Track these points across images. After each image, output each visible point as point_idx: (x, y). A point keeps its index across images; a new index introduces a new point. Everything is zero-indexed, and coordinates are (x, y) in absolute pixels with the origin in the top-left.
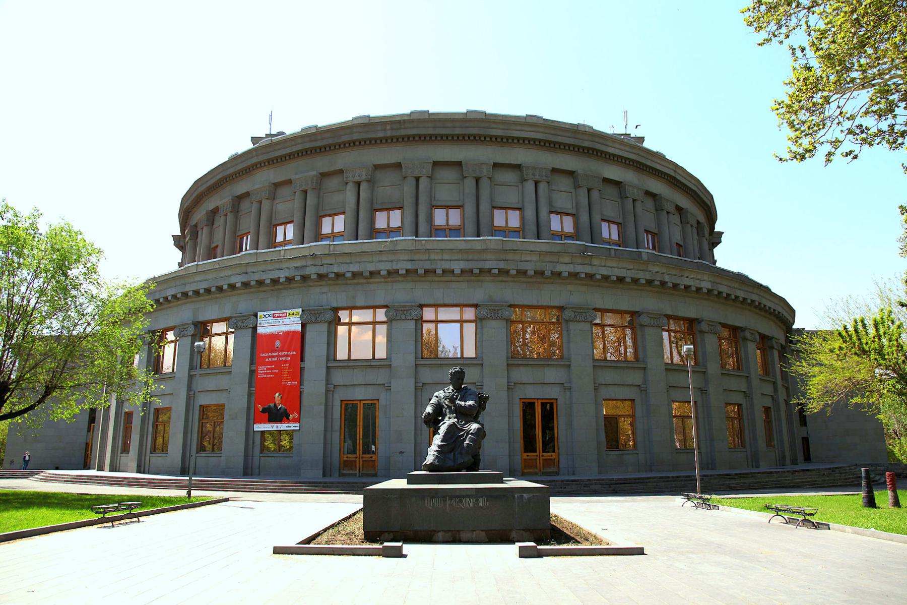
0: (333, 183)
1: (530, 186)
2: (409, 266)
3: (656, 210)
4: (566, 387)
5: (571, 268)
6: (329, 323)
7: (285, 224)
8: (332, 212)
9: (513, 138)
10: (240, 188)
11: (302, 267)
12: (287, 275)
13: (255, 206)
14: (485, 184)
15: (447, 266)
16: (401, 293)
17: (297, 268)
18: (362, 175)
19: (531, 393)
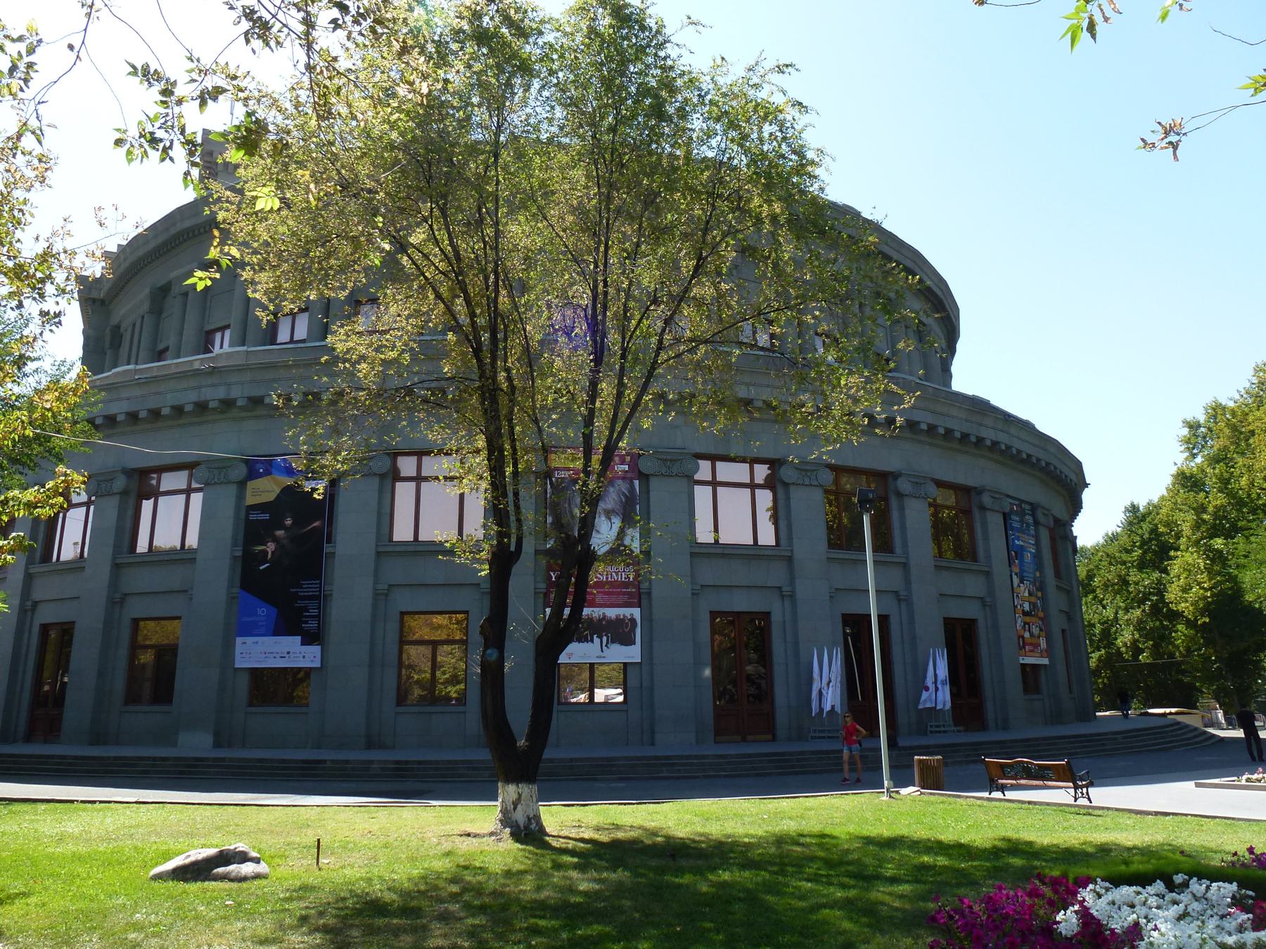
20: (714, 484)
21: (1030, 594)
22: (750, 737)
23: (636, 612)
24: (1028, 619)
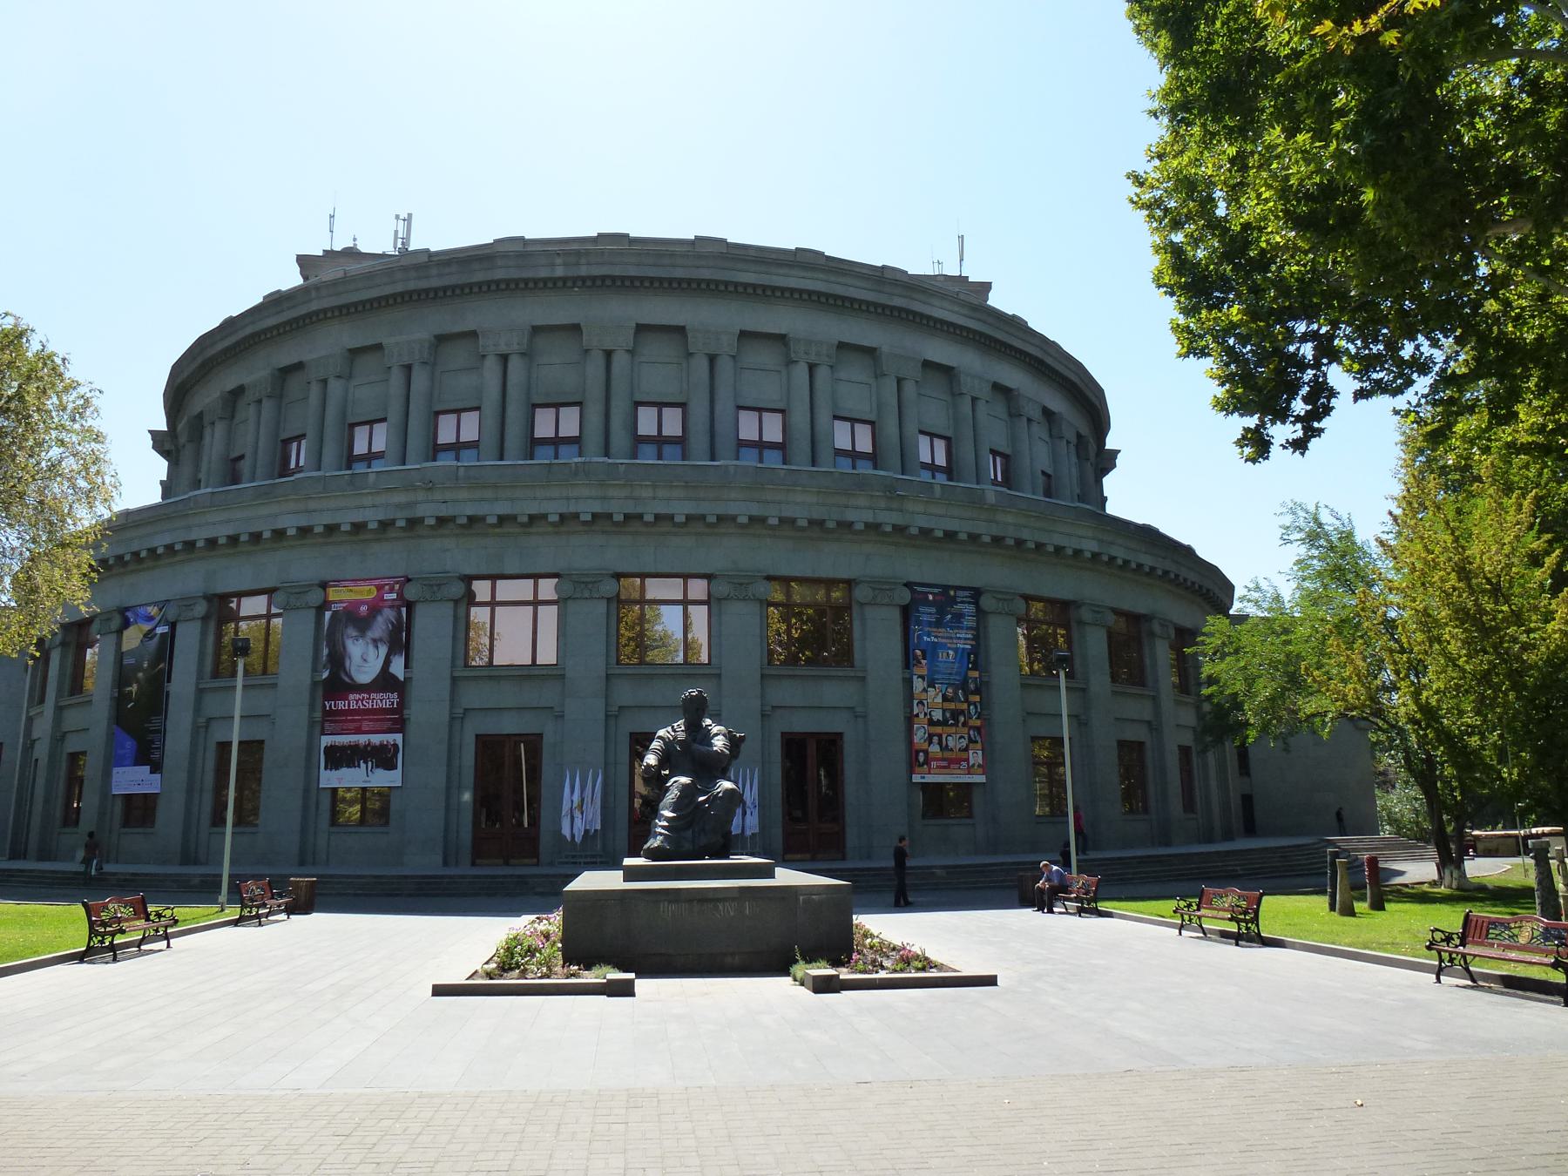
0: (457, 355)
1: (801, 371)
2: (597, 508)
3: (1010, 415)
4: (858, 714)
5: (868, 516)
6: (456, 602)
7: (371, 423)
8: (460, 405)
9: (774, 289)
10: (286, 355)
11: (410, 505)
12: (381, 517)
13: (315, 389)
14: (725, 367)
15: (662, 509)
16: (587, 553)
17: (399, 506)
18: (510, 342)
19: (802, 724)
20: (493, 604)
21: (945, 699)
22: (512, 861)
23: (398, 738)
24: (938, 730)
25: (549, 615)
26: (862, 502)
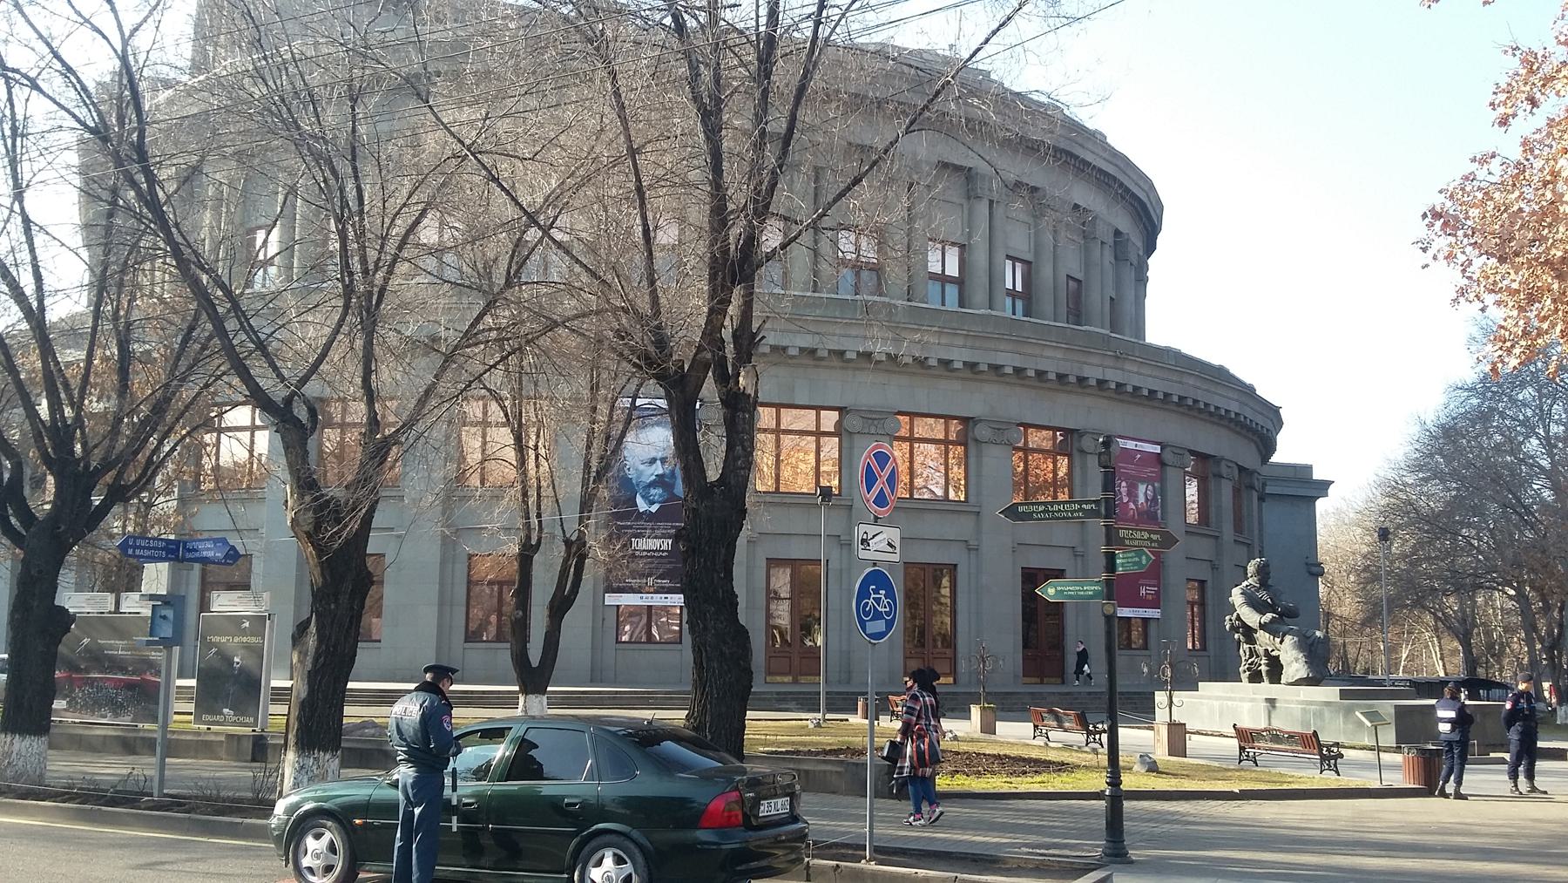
1: (983, 208)
16: (868, 391)
25: (831, 446)
26: (1095, 360)
